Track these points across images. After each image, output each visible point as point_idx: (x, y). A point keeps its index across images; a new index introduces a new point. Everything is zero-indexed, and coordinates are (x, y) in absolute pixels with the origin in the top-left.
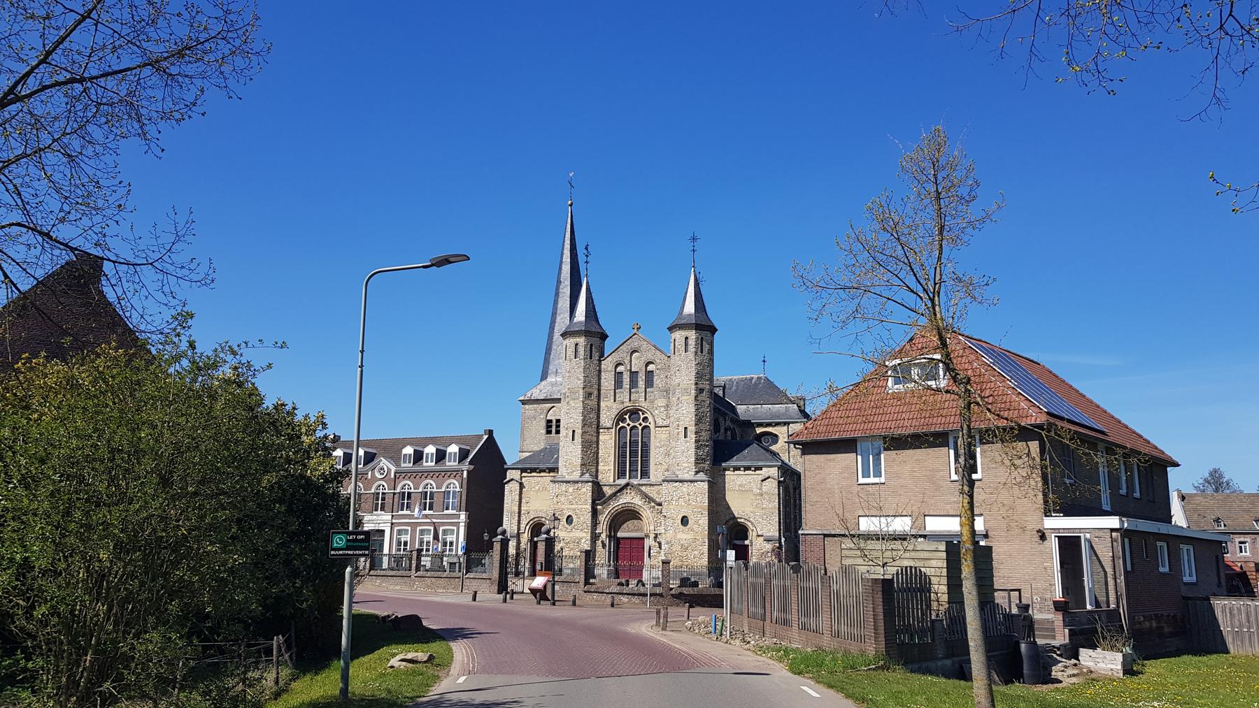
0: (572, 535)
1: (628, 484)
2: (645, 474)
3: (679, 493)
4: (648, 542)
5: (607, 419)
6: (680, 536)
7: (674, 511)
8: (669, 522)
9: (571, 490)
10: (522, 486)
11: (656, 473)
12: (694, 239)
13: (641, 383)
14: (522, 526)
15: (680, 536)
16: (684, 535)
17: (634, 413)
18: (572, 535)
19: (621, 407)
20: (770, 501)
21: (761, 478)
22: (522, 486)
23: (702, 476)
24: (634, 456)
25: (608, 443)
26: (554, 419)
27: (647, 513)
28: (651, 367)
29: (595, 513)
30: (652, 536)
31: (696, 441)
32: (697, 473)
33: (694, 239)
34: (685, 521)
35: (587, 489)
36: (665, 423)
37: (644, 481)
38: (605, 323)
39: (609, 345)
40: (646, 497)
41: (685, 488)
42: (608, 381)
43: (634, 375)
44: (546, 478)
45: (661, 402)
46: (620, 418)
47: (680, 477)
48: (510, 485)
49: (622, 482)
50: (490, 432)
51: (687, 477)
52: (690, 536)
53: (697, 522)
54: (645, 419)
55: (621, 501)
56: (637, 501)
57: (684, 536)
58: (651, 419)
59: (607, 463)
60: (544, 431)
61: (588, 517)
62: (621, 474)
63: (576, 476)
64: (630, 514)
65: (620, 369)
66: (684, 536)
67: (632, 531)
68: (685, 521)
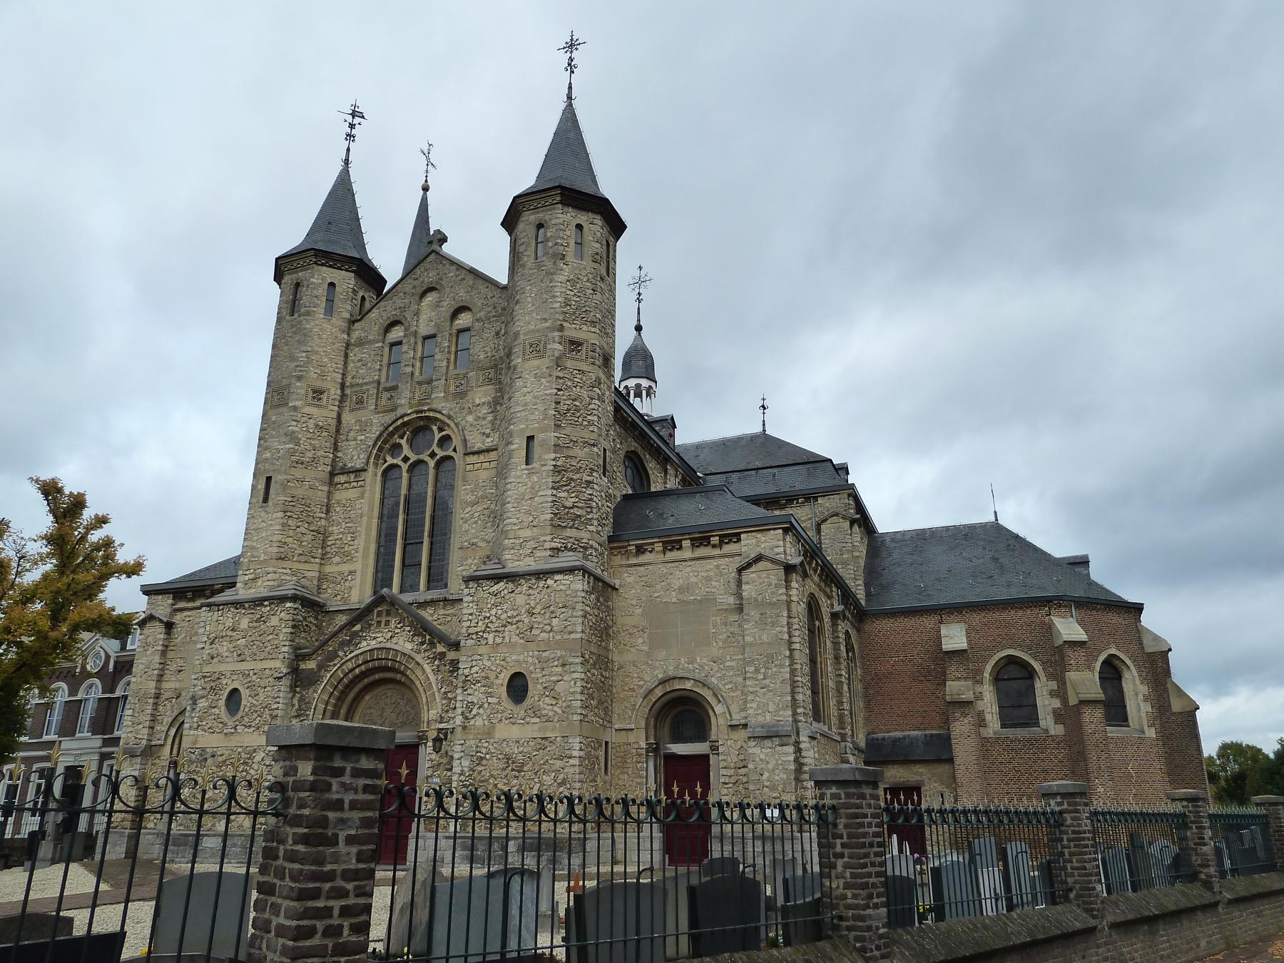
0: (234, 741)
3: (504, 612)
4: (427, 755)
6: (506, 731)
7: (487, 663)
8: (477, 694)
9: (244, 623)
12: (572, 45)
15: (506, 731)
16: (515, 731)
17: (420, 427)
18: (234, 741)
27: (426, 674)
33: (572, 45)
34: (518, 687)
36: (489, 442)
37: (434, 594)
40: (424, 631)
41: (522, 596)
46: (387, 443)
47: (512, 566)
51: (529, 564)
52: (533, 730)
53: (549, 690)
54: (445, 440)
56: (404, 643)
57: (515, 732)
58: (456, 441)
59: (347, 557)
64: (384, 676)
65: (396, 333)
66: (515, 732)
68: (518, 687)
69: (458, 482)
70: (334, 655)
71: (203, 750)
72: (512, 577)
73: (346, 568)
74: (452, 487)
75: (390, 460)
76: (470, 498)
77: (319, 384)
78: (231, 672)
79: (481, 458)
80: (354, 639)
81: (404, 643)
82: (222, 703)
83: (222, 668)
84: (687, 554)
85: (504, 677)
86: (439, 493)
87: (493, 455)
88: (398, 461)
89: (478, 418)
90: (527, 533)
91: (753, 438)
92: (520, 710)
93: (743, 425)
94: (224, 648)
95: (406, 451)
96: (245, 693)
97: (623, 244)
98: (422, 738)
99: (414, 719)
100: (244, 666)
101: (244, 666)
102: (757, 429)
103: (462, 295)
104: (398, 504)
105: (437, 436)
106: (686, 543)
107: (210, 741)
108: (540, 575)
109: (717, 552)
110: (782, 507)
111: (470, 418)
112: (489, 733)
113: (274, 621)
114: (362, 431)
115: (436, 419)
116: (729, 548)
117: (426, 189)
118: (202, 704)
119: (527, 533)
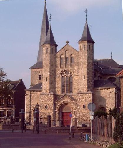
0: (47, 112)
1: (65, 95)
2: (71, 92)
5: (58, 74)
8: (79, 107)
9: (47, 97)
10: (30, 96)
11: (75, 91)
12: (86, 11)
13: (69, 62)
14: (32, 109)
15: (83, 111)
16: (84, 111)
17: (67, 71)
19: (62, 69)
20: (112, 99)
21: (110, 92)
22: (30, 96)
23: (90, 91)
24: (68, 86)
25: (59, 81)
26: (41, 74)
28: (73, 56)
29: (55, 105)
30: (74, 112)
31: (88, 80)
32: (88, 91)
33: (86, 11)
35: (52, 97)
37: (71, 94)
38: (57, 40)
39: (58, 49)
41: (84, 96)
42: (58, 61)
43: (66, 58)
44: (38, 94)
45: (76, 68)
48: (27, 96)
49: (63, 94)
50: (21, 80)
55: (63, 101)
56: (69, 100)
57: (84, 111)
60: (38, 79)
61: (52, 106)
62: (63, 92)
63: (48, 92)
66: (84, 111)
67: (67, 110)
69: (73, 80)
70: (59, 102)
71: (43, 113)
72: (83, 94)
73: (58, 90)
74: (72, 79)
75: (63, 75)
76: (75, 82)
77: (52, 64)
78: (46, 103)
79: (76, 76)
80: (62, 100)
81: (69, 100)
82: (45, 107)
83: (44, 103)
84: (103, 90)
85: (83, 105)
86: (70, 80)
87: (78, 76)
88: (64, 75)
89: (76, 71)
90: (85, 88)
91: (110, 60)
92: (85, 109)
93: (107, 57)
94: (44, 100)
95: (65, 74)
96: (48, 106)
97: (94, 45)
98: (72, 112)
99: (70, 109)
100: (47, 103)
101: (47, 103)
102: (110, 58)
103: (72, 52)
104: (64, 81)
105: (70, 73)
106: (103, 89)
107: (43, 111)
108: (86, 94)
109: (106, 90)
110: (114, 75)
111: (75, 71)
112: (81, 111)
113: (51, 97)
114: (58, 71)
115: (69, 70)
116: (109, 90)
117: (46, 2)
118: (42, 107)
119: (85, 88)
